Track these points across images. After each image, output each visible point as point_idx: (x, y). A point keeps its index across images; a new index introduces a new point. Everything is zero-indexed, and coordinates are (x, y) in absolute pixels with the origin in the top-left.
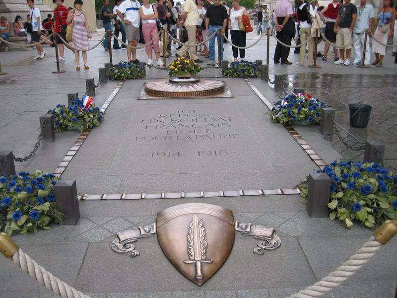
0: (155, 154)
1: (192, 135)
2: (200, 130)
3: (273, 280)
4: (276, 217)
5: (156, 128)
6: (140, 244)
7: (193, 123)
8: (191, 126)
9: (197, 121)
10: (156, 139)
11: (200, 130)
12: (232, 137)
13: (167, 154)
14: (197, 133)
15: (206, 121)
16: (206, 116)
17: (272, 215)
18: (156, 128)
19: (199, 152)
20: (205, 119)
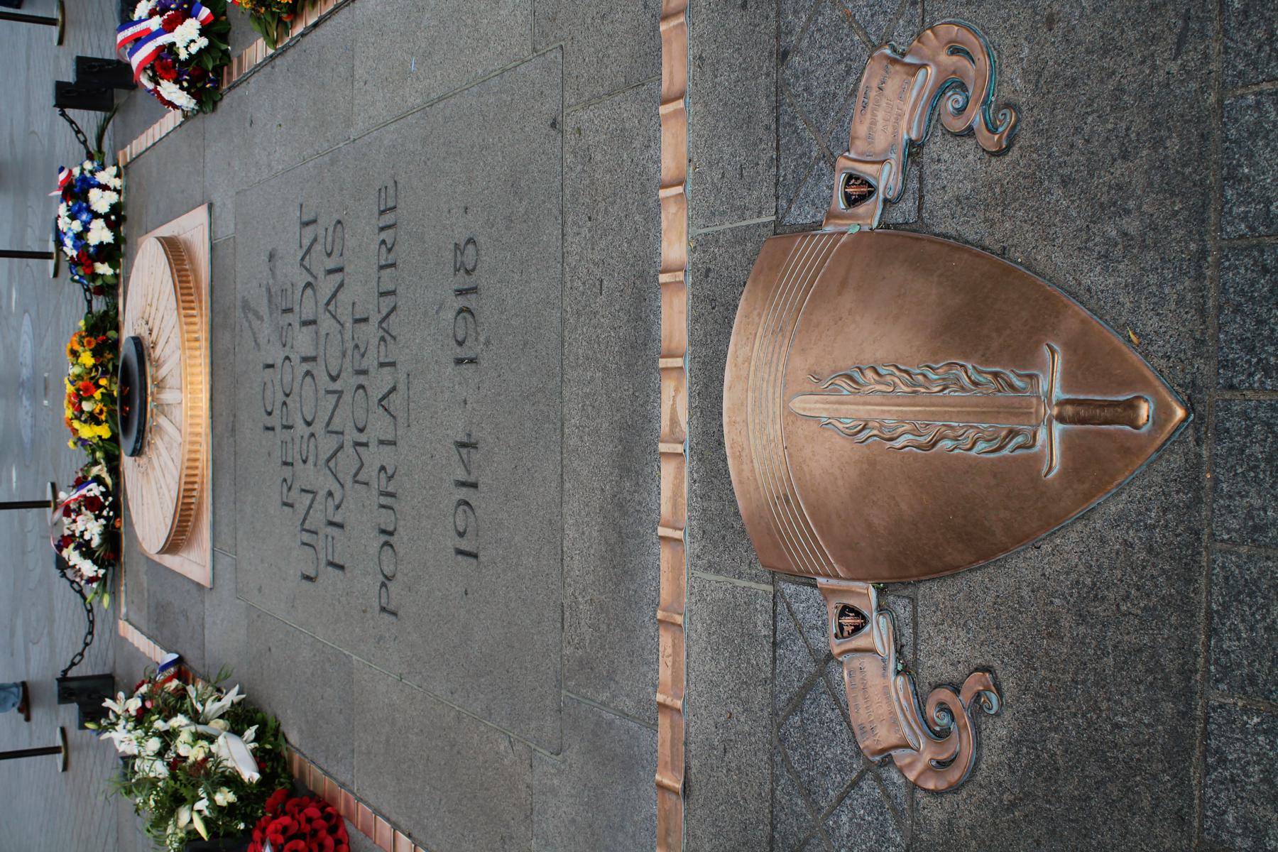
0: (465, 545)
1: (380, 382)
2: (357, 346)
3: (1174, 67)
4: (805, 43)
5: (340, 526)
6: (934, 666)
7: (323, 378)
8: (337, 386)
9: (314, 359)
10: (391, 534)
11: (357, 346)
12: (389, 219)
13: (463, 493)
14: (370, 362)
15: (314, 322)
16: (292, 318)
17: (796, 60)
18: (340, 526)
19: (459, 361)
20: (306, 323)
